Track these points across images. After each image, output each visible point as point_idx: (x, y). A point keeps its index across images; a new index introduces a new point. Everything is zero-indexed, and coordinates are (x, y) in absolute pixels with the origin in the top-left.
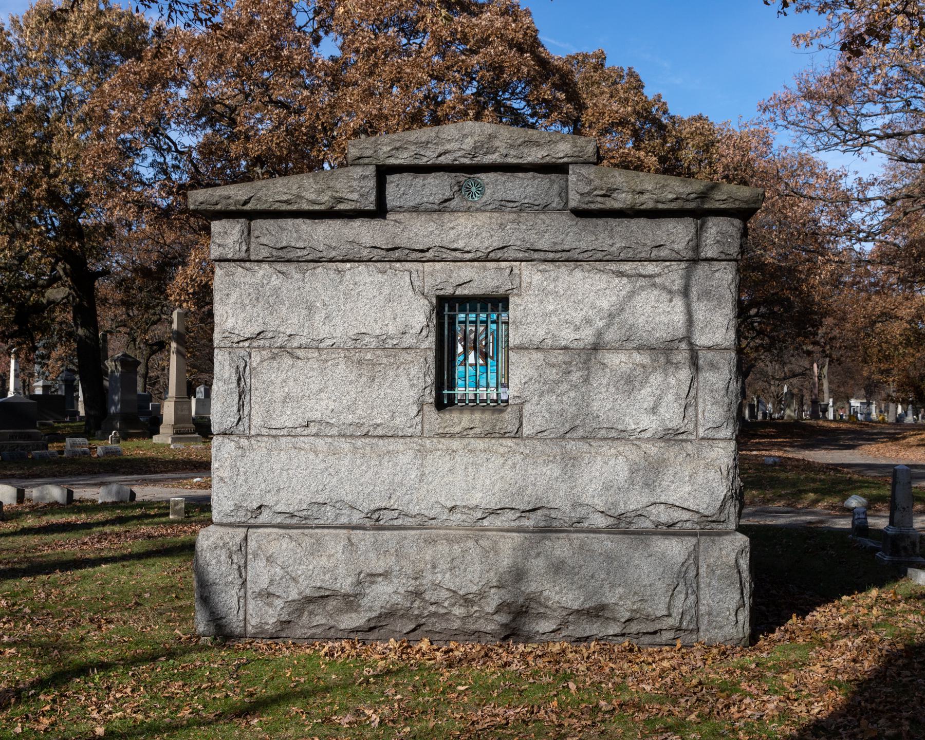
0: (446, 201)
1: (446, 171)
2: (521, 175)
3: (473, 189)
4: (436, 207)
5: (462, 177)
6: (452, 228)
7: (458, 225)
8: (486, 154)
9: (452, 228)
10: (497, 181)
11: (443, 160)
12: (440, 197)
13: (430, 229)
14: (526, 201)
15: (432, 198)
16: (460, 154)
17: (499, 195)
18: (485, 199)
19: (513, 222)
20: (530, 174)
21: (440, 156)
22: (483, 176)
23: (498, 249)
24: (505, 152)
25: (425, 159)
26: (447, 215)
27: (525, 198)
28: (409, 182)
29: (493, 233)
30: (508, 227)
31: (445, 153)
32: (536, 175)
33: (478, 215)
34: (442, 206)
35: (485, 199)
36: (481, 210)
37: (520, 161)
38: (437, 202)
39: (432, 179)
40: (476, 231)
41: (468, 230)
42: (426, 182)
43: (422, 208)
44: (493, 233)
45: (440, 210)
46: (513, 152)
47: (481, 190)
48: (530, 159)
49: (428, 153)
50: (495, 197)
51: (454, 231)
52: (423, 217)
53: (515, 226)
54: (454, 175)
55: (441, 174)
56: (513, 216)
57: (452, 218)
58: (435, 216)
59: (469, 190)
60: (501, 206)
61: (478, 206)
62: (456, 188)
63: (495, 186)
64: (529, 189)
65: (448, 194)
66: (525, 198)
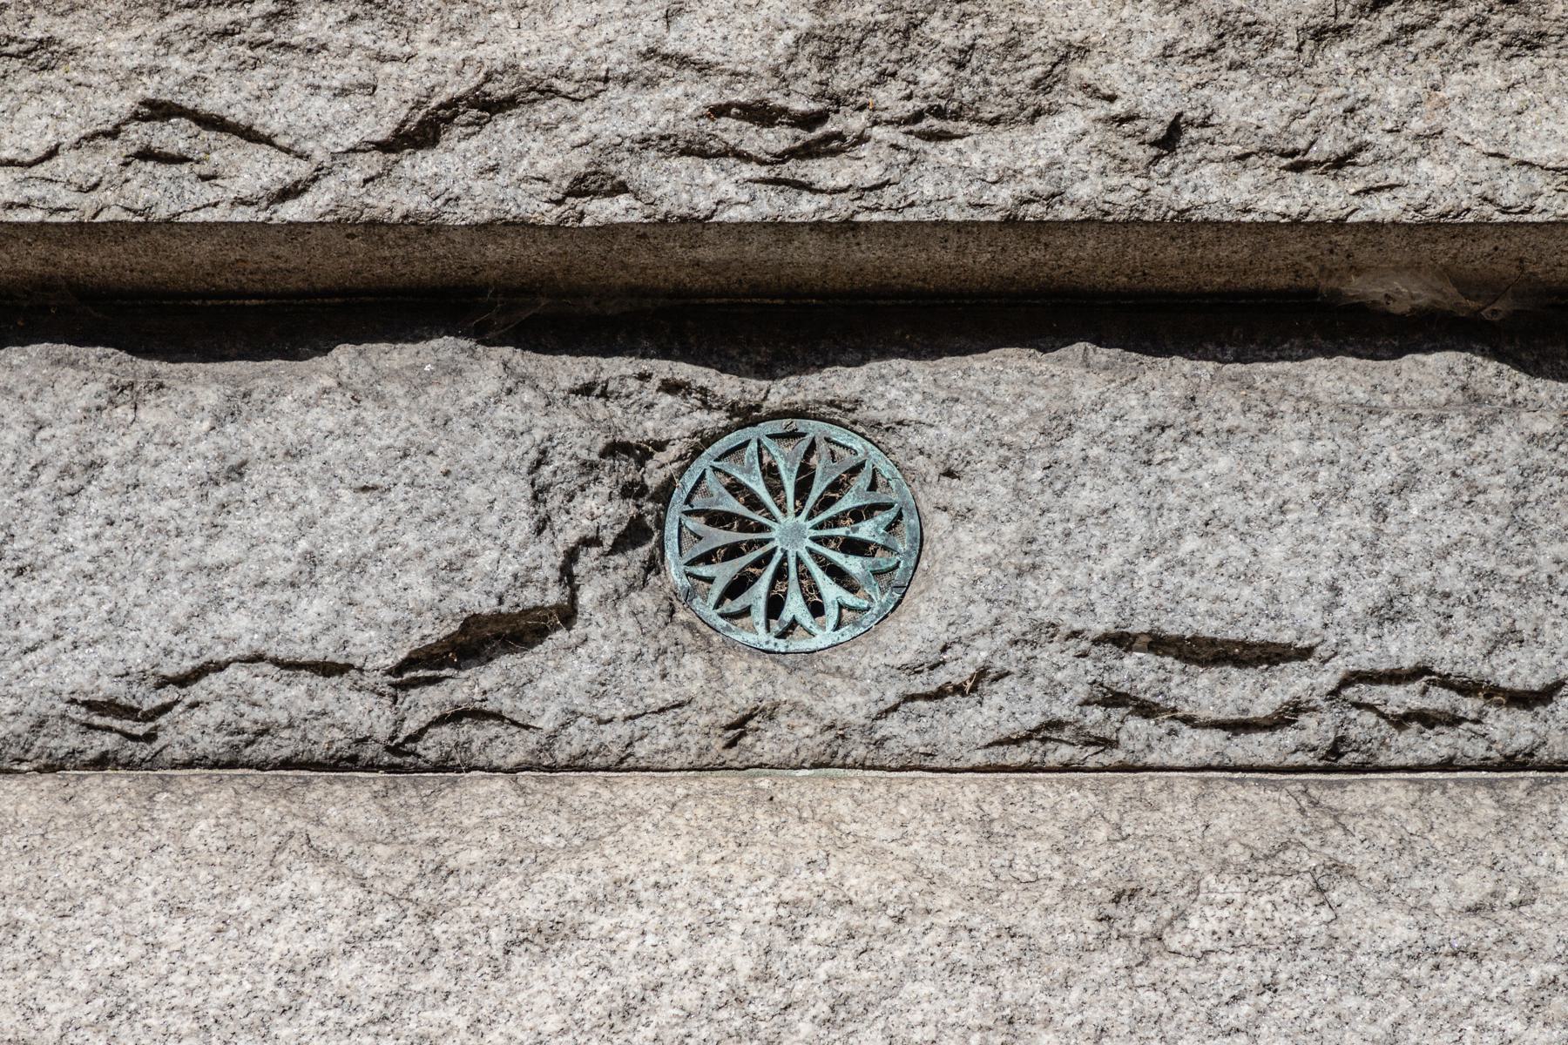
0: (477, 640)
1: (486, 335)
2: (1332, 377)
3: (791, 533)
4: (362, 713)
5: (657, 399)
6: (549, 936)
7: (621, 892)
8: (936, 121)
9: (549, 936)
10: (1059, 425)
11: (467, 181)
12: (408, 602)
13: (284, 940)
14: (1402, 648)
15: (313, 609)
16: (649, 111)
17: (1095, 581)
18: (919, 627)
19: (1266, 863)
20: (1432, 372)
21: (422, 133)
22: (893, 386)
23: (1380, 189)
24: (1158, 99)
25: (254, 171)
26: (483, 797)
27: (1388, 613)
28: (60, 441)
29: (1021, 988)
30: (1202, 926)
31: (487, 106)
32: (1489, 373)
33: (843, 795)
34: (427, 701)
35: (919, 627)
36: (880, 761)
37: (1327, 198)
38: (378, 650)
39: (314, 404)
40: (817, 962)
41: (732, 952)
42: (251, 436)
43: (195, 726)
44: (1021, 988)
45: (399, 758)
46: (1246, 105)
47: (870, 538)
48: (1438, 183)
49: (295, 105)
50: (1046, 597)
51: (564, 971)
52: (209, 811)
53: (1280, 909)
54: (571, 369)
55: (445, 347)
56: (1249, 814)
57: (548, 830)
58: (350, 804)
59: (742, 526)
60: (1140, 693)
61: (848, 703)
62: (599, 509)
63: (1040, 485)
64: (1427, 518)
65: (503, 566)
66: (1388, 613)
